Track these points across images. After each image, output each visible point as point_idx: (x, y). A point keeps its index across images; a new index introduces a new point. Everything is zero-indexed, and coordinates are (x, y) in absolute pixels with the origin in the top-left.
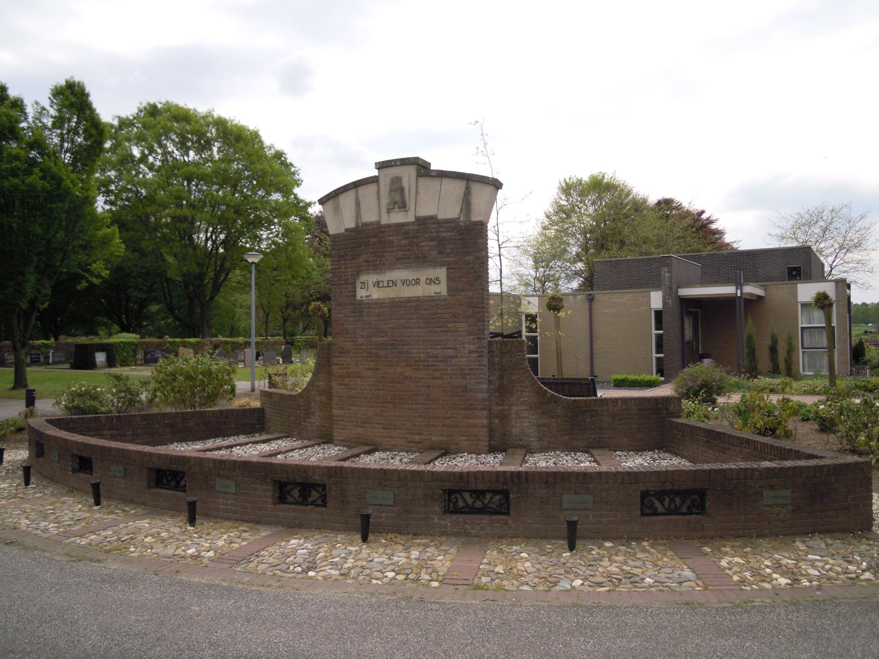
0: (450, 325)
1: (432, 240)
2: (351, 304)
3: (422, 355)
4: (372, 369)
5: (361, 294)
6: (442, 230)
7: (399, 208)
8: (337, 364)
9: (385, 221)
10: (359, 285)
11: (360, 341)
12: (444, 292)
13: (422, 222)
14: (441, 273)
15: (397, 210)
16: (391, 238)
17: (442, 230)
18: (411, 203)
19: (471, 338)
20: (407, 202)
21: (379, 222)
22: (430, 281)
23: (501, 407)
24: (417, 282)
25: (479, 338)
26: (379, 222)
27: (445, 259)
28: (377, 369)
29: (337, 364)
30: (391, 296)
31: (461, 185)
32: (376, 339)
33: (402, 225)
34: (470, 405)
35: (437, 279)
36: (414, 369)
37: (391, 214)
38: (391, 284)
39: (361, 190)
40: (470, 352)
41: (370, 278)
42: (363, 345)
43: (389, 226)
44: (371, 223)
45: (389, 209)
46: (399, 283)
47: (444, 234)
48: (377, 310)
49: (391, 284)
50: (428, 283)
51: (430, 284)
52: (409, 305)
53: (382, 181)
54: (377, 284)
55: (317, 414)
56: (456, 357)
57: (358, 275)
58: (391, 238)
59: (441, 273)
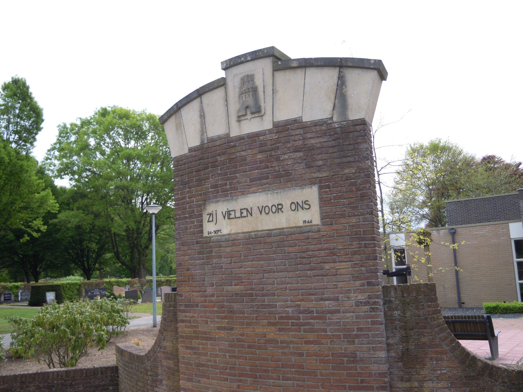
0: (327, 266)
1: (297, 150)
2: (197, 243)
3: (290, 310)
4: (224, 329)
5: (209, 228)
6: (309, 135)
7: (252, 113)
8: (183, 321)
9: (235, 132)
10: (205, 218)
11: (210, 290)
12: (317, 220)
13: (283, 128)
14: (311, 194)
15: (249, 116)
16: (243, 153)
17: (309, 135)
18: (266, 106)
19: (358, 283)
20: (262, 104)
21: (228, 135)
22: (297, 206)
23: (407, 385)
24: (279, 208)
25: (369, 284)
26: (228, 135)
27: (315, 175)
28: (232, 329)
29: (183, 321)
30: (245, 230)
31: (330, 76)
32: (229, 287)
33: (257, 135)
34: (362, 381)
35: (306, 202)
36: (280, 330)
37: (243, 122)
38: (245, 214)
39: (206, 98)
40: (359, 304)
41: (218, 208)
42: (213, 295)
43: (241, 138)
44: (219, 138)
45: (239, 117)
46: (255, 211)
47: (313, 141)
48: (228, 250)
49: (245, 214)
50: (294, 209)
51: (296, 209)
52: (269, 240)
53: (230, 84)
54: (228, 215)
55: (164, 382)
56: (338, 311)
57: (204, 204)
58: (243, 153)
59: (311, 194)
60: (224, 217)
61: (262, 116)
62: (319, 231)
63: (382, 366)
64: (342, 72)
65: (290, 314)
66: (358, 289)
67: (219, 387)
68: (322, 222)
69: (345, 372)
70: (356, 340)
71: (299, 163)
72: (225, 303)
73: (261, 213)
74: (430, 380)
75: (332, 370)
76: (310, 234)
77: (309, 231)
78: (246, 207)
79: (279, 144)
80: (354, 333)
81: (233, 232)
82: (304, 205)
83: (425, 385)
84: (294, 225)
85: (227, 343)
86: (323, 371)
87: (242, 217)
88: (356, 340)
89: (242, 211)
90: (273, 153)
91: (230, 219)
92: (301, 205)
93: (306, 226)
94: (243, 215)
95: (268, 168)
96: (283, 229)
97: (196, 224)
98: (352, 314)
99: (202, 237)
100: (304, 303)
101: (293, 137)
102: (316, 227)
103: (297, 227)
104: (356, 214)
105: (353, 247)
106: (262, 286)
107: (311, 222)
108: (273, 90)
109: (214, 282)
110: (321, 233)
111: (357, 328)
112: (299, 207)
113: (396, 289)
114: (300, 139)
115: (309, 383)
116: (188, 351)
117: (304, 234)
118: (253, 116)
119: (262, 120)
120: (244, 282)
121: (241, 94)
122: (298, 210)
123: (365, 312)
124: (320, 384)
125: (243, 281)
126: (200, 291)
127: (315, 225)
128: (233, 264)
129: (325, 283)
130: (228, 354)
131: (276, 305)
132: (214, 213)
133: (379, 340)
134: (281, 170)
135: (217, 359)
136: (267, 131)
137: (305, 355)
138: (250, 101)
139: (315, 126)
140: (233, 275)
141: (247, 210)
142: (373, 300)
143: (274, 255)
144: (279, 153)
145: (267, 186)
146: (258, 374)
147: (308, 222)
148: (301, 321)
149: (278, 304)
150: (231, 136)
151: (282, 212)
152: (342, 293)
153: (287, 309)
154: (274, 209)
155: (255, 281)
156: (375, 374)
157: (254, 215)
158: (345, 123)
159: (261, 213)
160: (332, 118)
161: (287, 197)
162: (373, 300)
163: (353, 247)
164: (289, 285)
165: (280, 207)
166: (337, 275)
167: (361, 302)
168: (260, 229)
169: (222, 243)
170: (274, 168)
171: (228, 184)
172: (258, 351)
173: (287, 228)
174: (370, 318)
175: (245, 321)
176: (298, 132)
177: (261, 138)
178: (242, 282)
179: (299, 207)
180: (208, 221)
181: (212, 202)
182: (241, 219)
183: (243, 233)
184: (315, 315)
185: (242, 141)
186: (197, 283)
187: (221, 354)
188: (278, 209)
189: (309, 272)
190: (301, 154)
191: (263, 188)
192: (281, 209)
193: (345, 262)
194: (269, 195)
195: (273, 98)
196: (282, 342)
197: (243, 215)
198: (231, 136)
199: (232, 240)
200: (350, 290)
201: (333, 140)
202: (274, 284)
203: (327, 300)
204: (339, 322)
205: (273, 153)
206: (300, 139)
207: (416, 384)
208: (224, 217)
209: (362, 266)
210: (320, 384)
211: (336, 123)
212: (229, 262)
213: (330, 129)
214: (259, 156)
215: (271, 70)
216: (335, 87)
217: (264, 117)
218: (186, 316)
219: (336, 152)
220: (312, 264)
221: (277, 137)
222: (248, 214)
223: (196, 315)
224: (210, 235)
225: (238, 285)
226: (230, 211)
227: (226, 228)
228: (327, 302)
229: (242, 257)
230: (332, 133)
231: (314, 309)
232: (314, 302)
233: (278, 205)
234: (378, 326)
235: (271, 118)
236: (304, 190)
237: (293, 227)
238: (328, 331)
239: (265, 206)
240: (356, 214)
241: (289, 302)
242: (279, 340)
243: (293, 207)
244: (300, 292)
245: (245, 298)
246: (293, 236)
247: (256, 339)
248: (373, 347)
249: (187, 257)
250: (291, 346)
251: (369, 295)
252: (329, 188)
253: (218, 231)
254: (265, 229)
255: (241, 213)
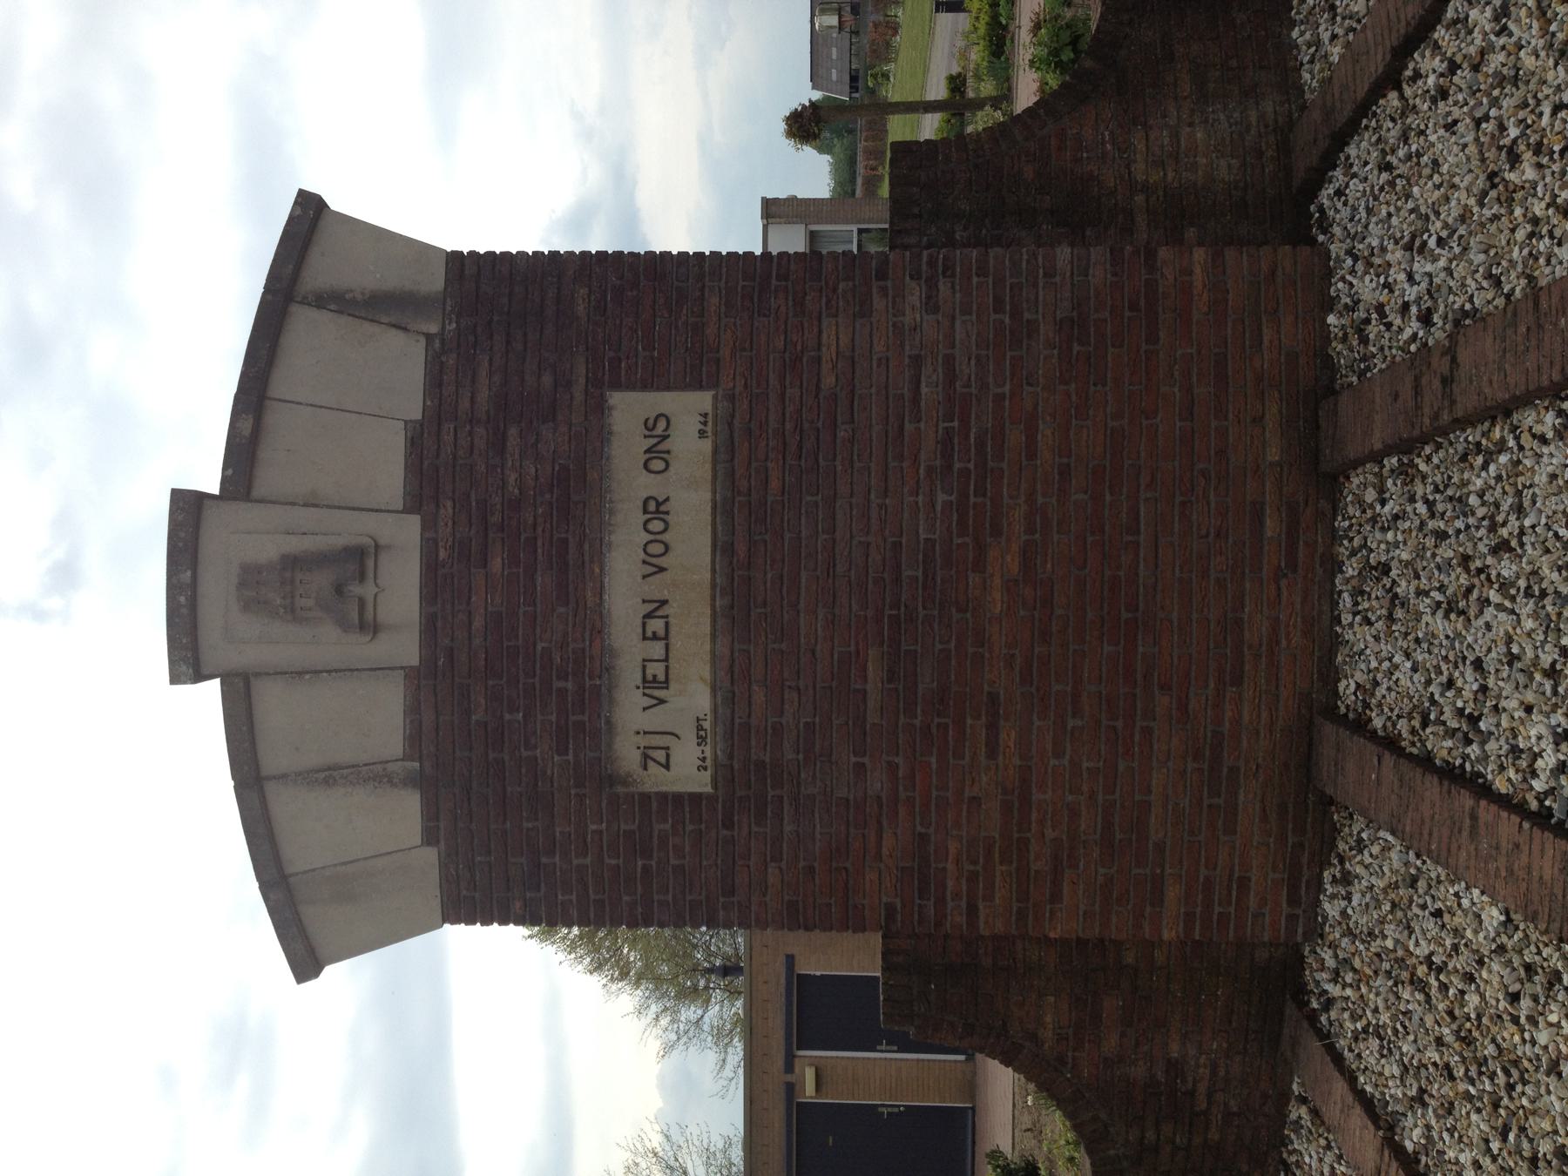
0: (829, 381)
1: (499, 444)
2: (729, 824)
3: (941, 497)
4: (993, 727)
5: (688, 770)
6: (465, 404)
7: (362, 577)
8: (972, 910)
9: (405, 647)
10: (656, 780)
11: (877, 782)
12: (703, 400)
13: (427, 484)
14: (628, 410)
15: (368, 590)
16: (478, 623)
17: (465, 404)
18: (347, 530)
19: (878, 303)
20: (340, 542)
21: (411, 674)
22: (657, 455)
23: (1141, 220)
24: (656, 509)
25: (882, 275)
26: (411, 674)
27: (579, 396)
28: (993, 698)
29: (972, 910)
30: (706, 627)
31: (304, 324)
32: (871, 704)
33: (431, 569)
34: (1133, 307)
35: (650, 426)
36: (997, 532)
37: (382, 616)
38: (656, 625)
39: (274, 759)
40: (931, 305)
41: (631, 713)
42: (892, 768)
43: (430, 627)
44: (413, 710)
45: (362, 627)
46: (655, 588)
47: (483, 395)
48: (759, 696)
49: (656, 625)
50: (665, 457)
51: (665, 457)
52: (741, 549)
53: (246, 657)
54: (655, 685)
55: (1175, 1050)
56: (949, 360)
57: (612, 780)
58: (478, 623)
59: (628, 410)
60: (662, 701)
61: (377, 546)
62: (732, 398)
63: (1093, 257)
64: (305, 298)
65: (953, 498)
66: (894, 302)
67: (1170, 764)
68: (708, 388)
69: (1111, 350)
70: (1027, 316)
71: (537, 441)
72: (917, 722)
73: (662, 570)
74: (1128, 166)
75: (1104, 385)
76: (736, 422)
77: (730, 424)
78: (639, 621)
79: (473, 496)
80: (1007, 320)
81: (707, 675)
82: (658, 429)
83: (1140, 178)
84: (708, 466)
85: (1037, 723)
86: (1109, 410)
87: (666, 637)
88: (1027, 316)
89: (649, 634)
90: (495, 519)
91: (667, 681)
92: (654, 441)
93: (715, 434)
94: (661, 633)
95: (535, 539)
96: (714, 502)
97: (668, 826)
98: (958, 323)
99: (711, 799)
100: (923, 456)
101: (461, 453)
102: (720, 405)
103: (715, 462)
104: (698, 294)
105: (783, 309)
106: (870, 586)
107: (706, 415)
108: (306, 505)
109: (853, 759)
110: (737, 390)
111: (996, 312)
112: (660, 447)
113: (899, 232)
114: (470, 433)
115: (1143, 454)
116: (1066, 889)
117: (736, 440)
118: (371, 574)
119: (389, 547)
120: (857, 644)
121: (293, 611)
122: (668, 452)
123: (953, 287)
124: (1145, 423)
125: (853, 648)
126: (879, 823)
127: (715, 407)
128: (801, 683)
129: (873, 390)
130: (1071, 723)
131: (926, 540)
132: (644, 741)
133: (1028, 261)
134: (548, 496)
135: (1085, 765)
136: (427, 535)
137: (1065, 460)
138: (322, 580)
139: (440, 385)
140: (834, 684)
141: (648, 616)
142: (924, 267)
143: (787, 536)
144: (498, 500)
145: (586, 547)
146: (1125, 615)
147: (705, 423)
148: (971, 466)
149: (923, 536)
150: (415, 662)
151: (667, 499)
152: (902, 345)
153: (939, 508)
154: (656, 526)
155: (855, 607)
156: (1115, 274)
157: (665, 595)
158: (449, 302)
159: (662, 570)
160: (429, 337)
161: (630, 481)
162: (924, 267)
163: (783, 309)
164: (873, 496)
165: (652, 506)
166: (853, 358)
167: (929, 298)
168: (708, 576)
169: (737, 721)
170: (540, 520)
171: (561, 684)
172: (1059, 612)
173: (714, 492)
174: (969, 278)
175: (971, 650)
176: (448, 438)
177: (442, 554)
178: (858, 652)
179: (660, 447)
180: (667, 767)
181: (610, 746)
182: (672, 640)
183: (714, 636)
184: (956, 424)
185: (439, 624)
186: (852, 830)
187: (1068, 752)
188: (657, 511)
189: (841, 434)
190: (513, 431)
191: (592, 561)
192: (659, 504)
193: (820, 332)
194: (613, 537)
195: (328, 507)
196: (1030, 530)
197: (661, 633)
198: (415, 662)
199: (732, 681)
200: (894, 325)
201: (491, 337)
202: (869, 544)
203: (918, 387)
204: (978, 358)
205: (495, 519)
206: (470, 433)
207: (1139, 199)
208: (662, 701)
209: (835, 290)
210: (1145, 423)
211: (443, 328)
212: (795, 695)
213: (459, 345)
214: (496, 564)
215: (244, 505)
216: (344, 319)
217: (382, 542)
218: (957, 896)
219: (525, 335)
220: (820, 425)
221: (449, 504)
222: (659, 613)
223: (953, 847)
224: (709, 762)
225: (865, 669)
226: (644, 680)
227: (694, 697)
228: (924, 390)
229: (784, 646)
230: (471, 338)
231: (942, 425)
232: (922, 425)
233: (645, 512)
234: (992, 262)
235: (391, 518)
236: (615, 428)
237: (714, 470)
238: (999, 390)
239: (642, 555)
240: (698, 294)
241: (920, 498)
242: (1024, 538)
243: (658, 465)
244: (893, 464)
245: (904, 647)
246: (737, 476)
247: (1022, 613)
248: (1045, 275)
249: (773, 876)
250: (1040, 500)
251: (912, 277)
252: (620, 360)
253: (700, 728)
254: (708, 559)
255: (655, 637)
